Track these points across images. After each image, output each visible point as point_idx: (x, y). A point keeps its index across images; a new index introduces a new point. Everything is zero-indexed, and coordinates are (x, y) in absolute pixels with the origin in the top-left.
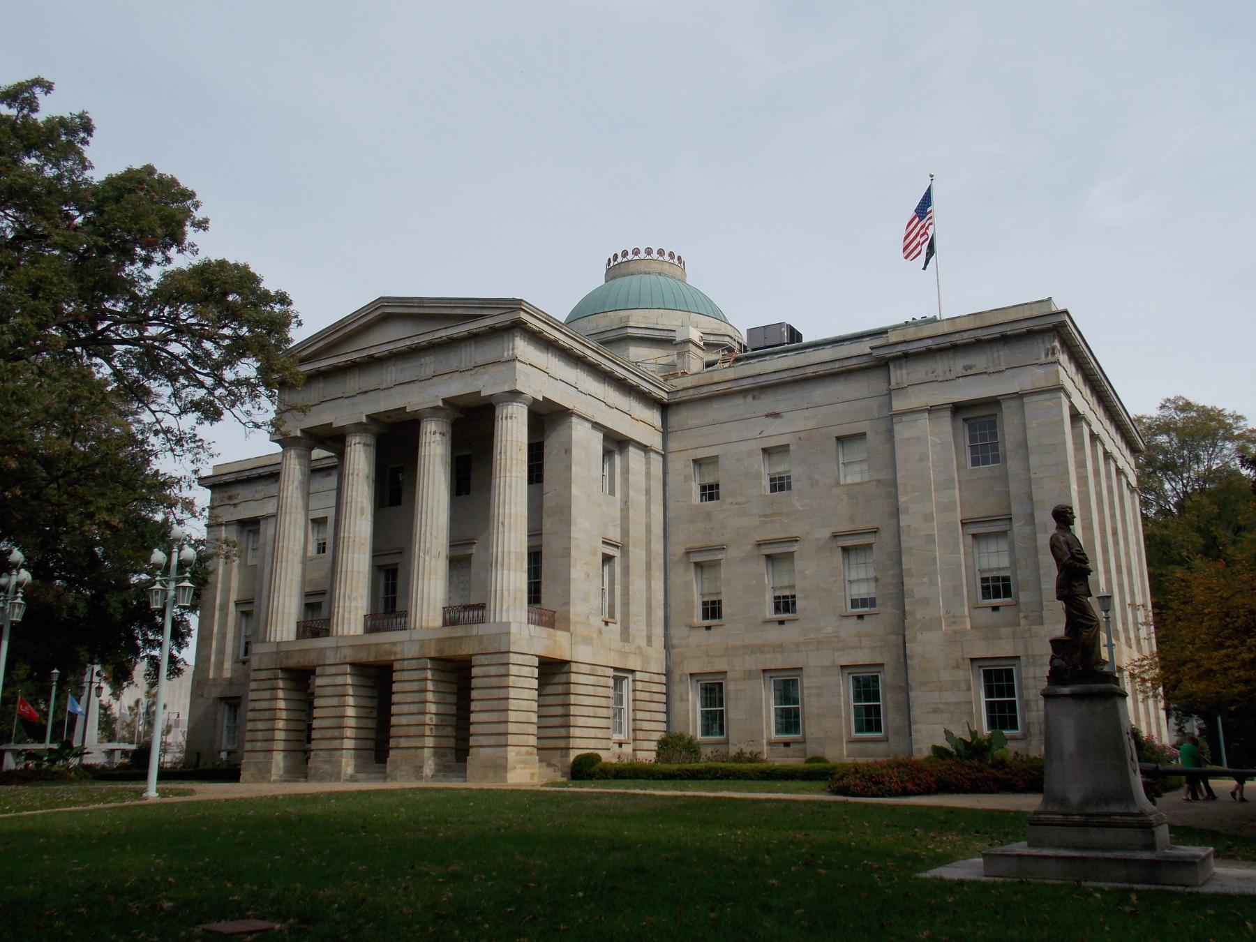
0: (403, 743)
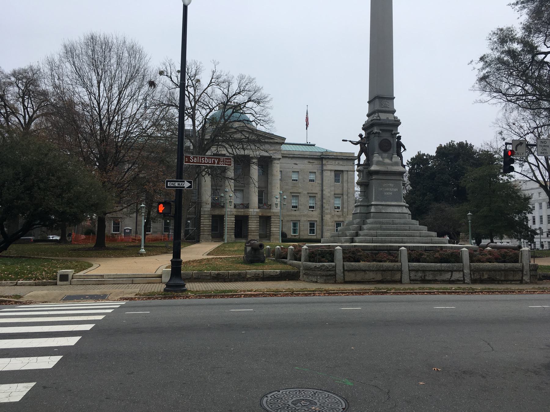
0: (252, 234)
